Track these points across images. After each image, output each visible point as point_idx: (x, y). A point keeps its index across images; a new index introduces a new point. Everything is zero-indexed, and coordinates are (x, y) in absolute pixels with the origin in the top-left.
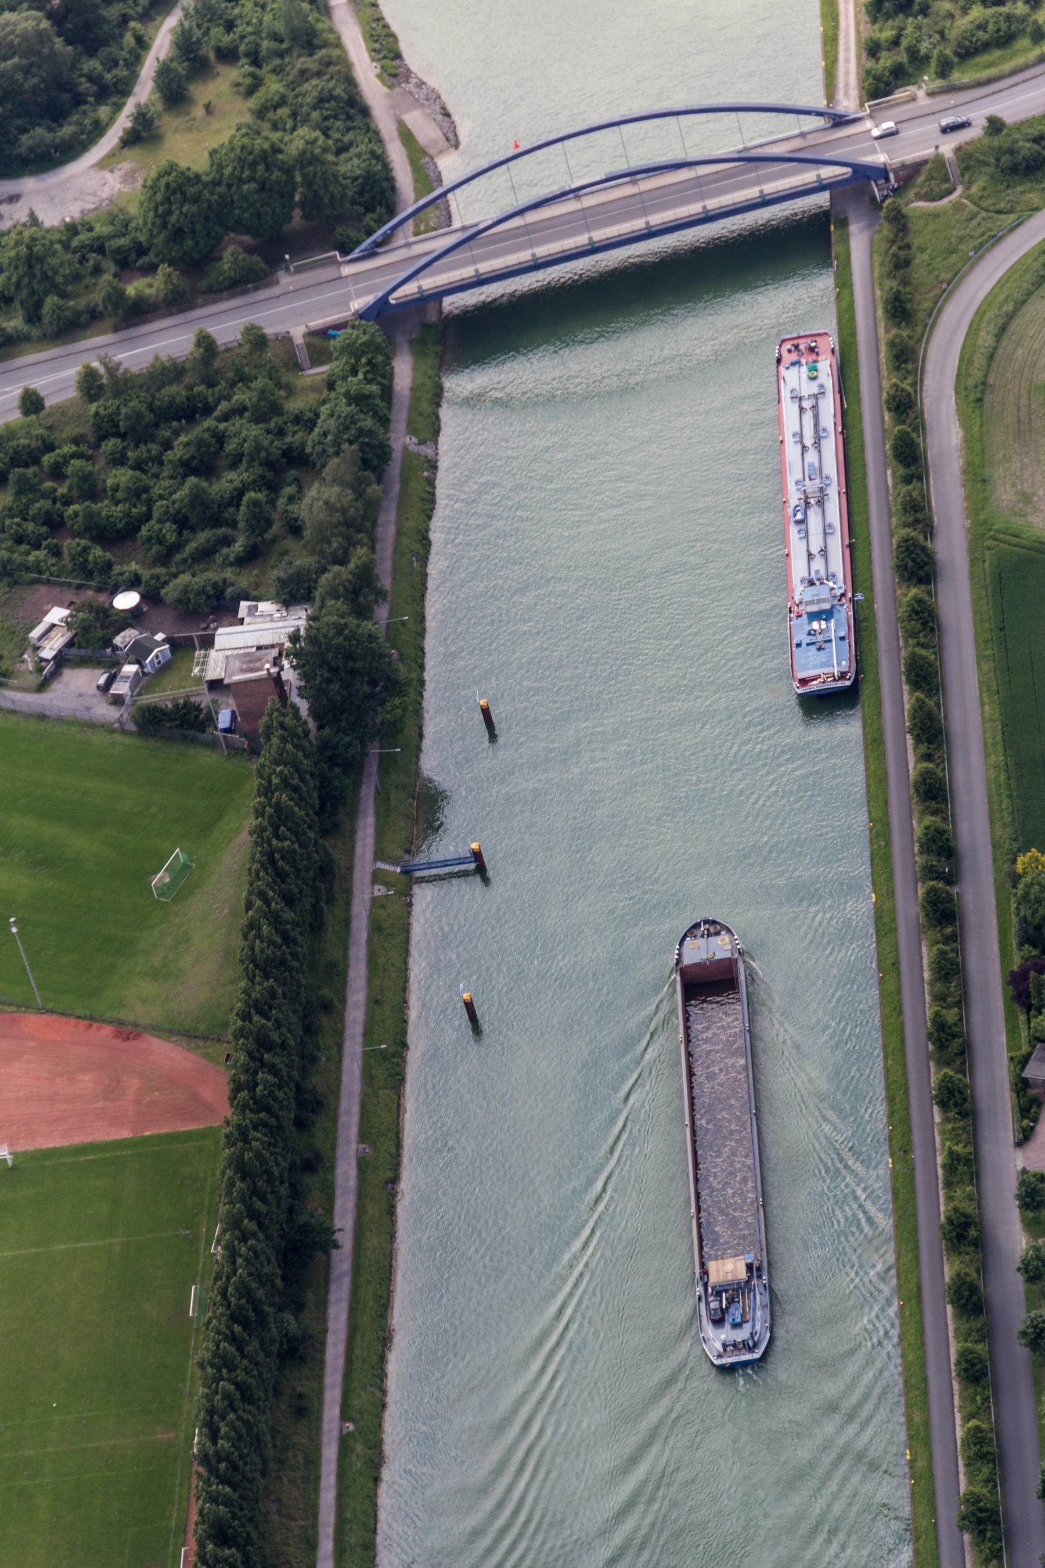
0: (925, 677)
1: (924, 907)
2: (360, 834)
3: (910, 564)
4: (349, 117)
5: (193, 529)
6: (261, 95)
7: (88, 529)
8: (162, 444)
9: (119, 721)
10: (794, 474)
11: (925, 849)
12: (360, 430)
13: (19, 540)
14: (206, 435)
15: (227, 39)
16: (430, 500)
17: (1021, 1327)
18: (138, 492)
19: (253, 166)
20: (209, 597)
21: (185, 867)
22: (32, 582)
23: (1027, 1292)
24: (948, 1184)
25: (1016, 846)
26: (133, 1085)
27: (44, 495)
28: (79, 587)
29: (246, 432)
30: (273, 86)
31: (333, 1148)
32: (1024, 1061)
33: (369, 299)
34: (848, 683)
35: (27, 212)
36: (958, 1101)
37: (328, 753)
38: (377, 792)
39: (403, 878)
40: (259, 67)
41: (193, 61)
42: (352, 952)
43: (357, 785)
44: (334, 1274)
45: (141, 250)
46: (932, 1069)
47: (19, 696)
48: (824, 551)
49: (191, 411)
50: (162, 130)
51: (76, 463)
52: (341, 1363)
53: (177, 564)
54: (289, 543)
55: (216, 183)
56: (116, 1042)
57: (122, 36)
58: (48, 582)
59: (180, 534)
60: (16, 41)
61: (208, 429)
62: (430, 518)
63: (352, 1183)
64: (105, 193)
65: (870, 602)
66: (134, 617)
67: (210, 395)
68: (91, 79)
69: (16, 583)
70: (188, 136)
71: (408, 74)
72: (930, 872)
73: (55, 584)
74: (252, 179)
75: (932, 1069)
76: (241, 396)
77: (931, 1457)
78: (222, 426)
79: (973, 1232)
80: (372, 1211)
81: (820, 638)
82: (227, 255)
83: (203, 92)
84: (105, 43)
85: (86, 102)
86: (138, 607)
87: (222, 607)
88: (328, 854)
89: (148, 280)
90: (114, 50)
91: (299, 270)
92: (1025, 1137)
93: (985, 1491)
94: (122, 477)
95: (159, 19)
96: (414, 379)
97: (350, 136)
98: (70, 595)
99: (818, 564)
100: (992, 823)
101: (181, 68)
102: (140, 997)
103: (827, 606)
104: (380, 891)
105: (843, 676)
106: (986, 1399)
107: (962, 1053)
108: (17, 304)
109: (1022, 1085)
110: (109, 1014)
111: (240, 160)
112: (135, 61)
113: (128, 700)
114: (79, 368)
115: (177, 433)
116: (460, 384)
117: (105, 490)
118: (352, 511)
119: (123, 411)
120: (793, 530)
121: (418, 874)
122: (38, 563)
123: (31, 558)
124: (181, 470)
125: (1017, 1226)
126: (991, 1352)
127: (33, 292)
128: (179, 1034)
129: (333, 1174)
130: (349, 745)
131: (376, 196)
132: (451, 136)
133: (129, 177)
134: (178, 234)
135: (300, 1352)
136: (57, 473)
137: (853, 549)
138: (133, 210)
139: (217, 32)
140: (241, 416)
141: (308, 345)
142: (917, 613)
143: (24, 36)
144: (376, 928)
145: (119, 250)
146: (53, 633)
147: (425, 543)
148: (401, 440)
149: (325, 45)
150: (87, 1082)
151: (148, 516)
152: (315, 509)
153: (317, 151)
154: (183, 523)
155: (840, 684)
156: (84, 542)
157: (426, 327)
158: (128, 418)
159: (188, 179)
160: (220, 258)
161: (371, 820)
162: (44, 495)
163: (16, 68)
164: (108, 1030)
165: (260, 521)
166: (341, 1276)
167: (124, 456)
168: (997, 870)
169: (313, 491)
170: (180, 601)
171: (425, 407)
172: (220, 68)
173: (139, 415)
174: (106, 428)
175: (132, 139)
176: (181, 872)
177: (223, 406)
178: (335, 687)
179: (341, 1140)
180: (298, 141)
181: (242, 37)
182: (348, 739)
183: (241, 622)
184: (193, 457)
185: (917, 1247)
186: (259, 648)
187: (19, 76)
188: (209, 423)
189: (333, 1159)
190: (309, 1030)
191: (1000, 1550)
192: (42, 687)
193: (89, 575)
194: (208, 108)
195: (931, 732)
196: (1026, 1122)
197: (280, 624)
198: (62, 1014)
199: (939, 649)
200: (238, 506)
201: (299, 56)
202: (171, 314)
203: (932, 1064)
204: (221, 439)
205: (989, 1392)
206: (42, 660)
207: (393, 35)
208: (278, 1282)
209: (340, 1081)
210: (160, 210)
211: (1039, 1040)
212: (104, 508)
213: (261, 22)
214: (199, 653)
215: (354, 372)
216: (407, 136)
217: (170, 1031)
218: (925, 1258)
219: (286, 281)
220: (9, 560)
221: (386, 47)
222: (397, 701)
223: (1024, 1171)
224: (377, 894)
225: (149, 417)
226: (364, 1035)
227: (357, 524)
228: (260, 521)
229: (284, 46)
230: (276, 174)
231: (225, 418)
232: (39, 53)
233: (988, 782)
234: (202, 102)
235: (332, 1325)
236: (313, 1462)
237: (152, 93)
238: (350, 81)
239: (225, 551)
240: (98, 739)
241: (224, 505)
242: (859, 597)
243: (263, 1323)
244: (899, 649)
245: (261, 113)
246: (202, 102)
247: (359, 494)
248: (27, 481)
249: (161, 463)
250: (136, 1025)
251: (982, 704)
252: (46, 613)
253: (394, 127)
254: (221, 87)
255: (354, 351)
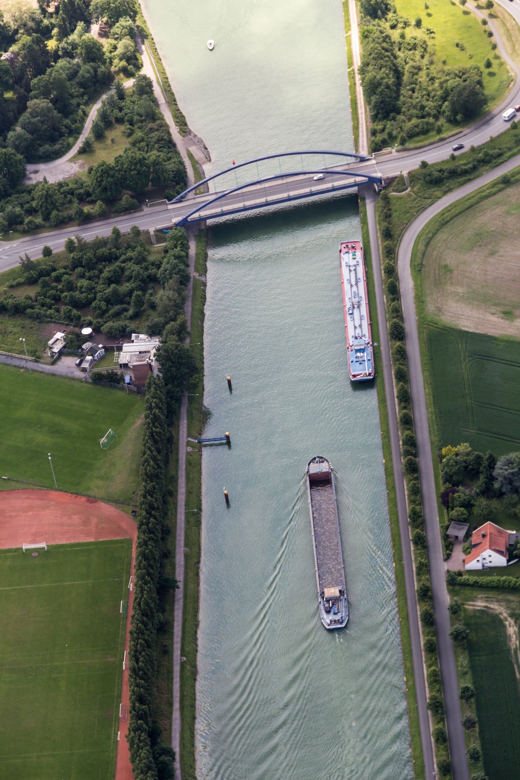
0: (402, 376)
1: (406, 466)
2: (181, 427)
3: (396, 333)
4: (169, 148)
5: (112, 304)
6: (134, 136)
7: (71, 302)
8: (99, 271)
9: (85, 378)
10: (348, 295)
11: (405, 443)
12: (180, 269)
13: (43, 305)
14: (117, 268)
15: (120, 115)
16: (204, 298)
17: (451, 632)
18: (91, 289)
19: (136, 164)
20: (120, 331)
21: (113, 436)
22: (48, 322)
23: (451, 617)
24: (418, 574)
25: (440, 444)
26: (94, 521)
27: (53, 288)
28: (67, 325)
29: (133, 268)
30: (139, 134)
31: (175, 549)
32: (447, 528)
33: (180, 219)
34: (372, 377)
35: (43, 177)
36: (421, 542)
37: (170, 395)
38: (188, 411)
39: (199, 445)
40: (133, 126)
41: (106, 122)
42: (180, 472)
43: (180, 407)
44: (176, 598)
45: (88, 194)
46: (410, 529)
47: (44, 366)
48: (360, 326)
49: (110, 259)
50: (94, 149)
51: (66, 276)
52: (180, 633)
53: (106, 318)
54: (150, 312)
55: (120, 170)
56: (87, 504)
57: (77, 111)
58: (55, 322)
59: (107, 306)
60: (39, 111)
61: (118, 266)
62: (204, 305)
63: (182, 563)
64: (73, 171)
65: (379, 346)
66: (89, 338)
67: (118, 253)
68: (66, 127)
69: (42, 322)
70: (105, 151)
71: (190, 132)
72: (407, 453)
73: (58, 323)
74: (135, 169)
75: (410, 529)
76: (130, 254)
77: (414, 681)
78: (123, 265)
79: (430, 594)
80: (191, 574)
81: (361, 359)
82: (124, 198)
83: (111, 134)
84: (71, 113)
85: (64, 136)
86: (91, 333)
87: (125, 335)
88: (172, 434)
89: (91, 206)
90: (75, 116)
91: (151, 206)
92: (448, 558)
93: (438, 695)
94: (84, 282)
95: (91, 105)
96: (197, 251)
97: (170, 155)
98: (63, 328)
99: (358, 330)
100: (430, 435)
101: (102, 124)
102: (96, 486)
103: (363, 347)
104: (190, 449)
105: (370, 374)
106: (436, 659)
107: (422, 523)
108: (40, 213)
109: (446, 537)
110: (84, 493)
111: (130, 162)
112: (83, 121)
113: (88, 370)
114: (66, 239)
115: (104, 267)
116: (215, 253)
117: (77, 287)
118: (178, 301)
119: (85, 257)
120: (348, 317)
121: (204, 443)
122: (51, 314)
123: (48, 312)
124: (107, 281)
125: (446, 592)
126: (437, 640)
127: (47, 209)
128: (112, 501)
129: (175, 559)
130: (178, 392)
131: (180, 179)
132: (208, 157)
133: (82, 166)
134: (105, 189)
135: (164, 628)
136: (58, 279)
137: (371, 325)
138: (84, 179)
139: (116, 111)
140: (130, 261)
141: (156, 235)
142: (399, 352)
143: (43, 110)
144: (189, 463)
145: (79, 194)
146: (57, 342)
147: (203, 314)
148: (193, 274)
149: (159, 119)
150: (76, 519)
151: (95, 299)
152: (163, 299)
153: (160, 160)
154: (108, 301)
155: (368, 378)
156: (70, 307)
157: (201, 230)
158: (86, 259)
159: (110, 168)
160: (121, 199)
161: (185, 421)
162: (53, 288)
163: (39, 121)
164: (84, 499)
165: (140, 303)
166: (179, 599)
167: (84, 274)
168: (433, 453)
169: (161, 292)
170: (108, 332)
171: (201, 262)
172: (117, 125)
173: (91, 259)
174: (76, 264)
175: (83, 151)
176: (111, 438)
177: (123, 257)
178: (174, 369)
179: (177, 546)
180: (153, 155)
181: (126, 114)
182: (178, 389)
183: (133, 342)
184: (112, 276)
185: (406, 598)
186: (140, 352)
187: (40, 125)
188: (118, 263)
189: (175, 553)
190: (165, 502)
191: (444, 718)
192: (53, 363)
193: (72, 320)
194: (113, 141)
195: (405, 398)
196: (448, 551)
197: (148, 343)
198: (66, 492)
199: (407, 365)
200: (131, 297)
201: (149, 123)
202: (101, 220)
203: (409, 527)
204: (123, 270)
205: (437, 656)
206: (53, 352)
207: (184, 117)
208: (157, 601)
209: (176, 522)
210: (99, 179)
211: (452, 520)
212: (77, 294)
213: (133, 109)
214: (116, 353)
215: (176, 247)
216: (191, 156)
217: (109, 500)
218: (409, 603)
219: (146, 210)
220: (40, 313)
221: (181, 121)
222: (197, 376)
223: (448, 571)
224: (189, 450)
225: (95, 260)
226: (185, 505)
227: (178, 307)
228: (140, 303)
229: (143, 118)
230: (144, 168)
231: (124, 262)
232: (48, 116)
233: (428, 419)
234: (110, 139)
235: (176, 618)
236: (170, 672)
237: (90, 133)
238: (169, 134)
239: (125, 313)
240: (76, 384)
241: (125, 296)
242: (376, 344)
243: (153, 617)
244: (391, 365)
245: (134, 144)
246: (110, 139)
247: (180, 294)
248: (47, 282)
249: (99, 278)
250: (95, 497)
251: (425, 389)
252: (55, 334)
253: (185, 152)
254: (117, 132)
255: (176, 238)
